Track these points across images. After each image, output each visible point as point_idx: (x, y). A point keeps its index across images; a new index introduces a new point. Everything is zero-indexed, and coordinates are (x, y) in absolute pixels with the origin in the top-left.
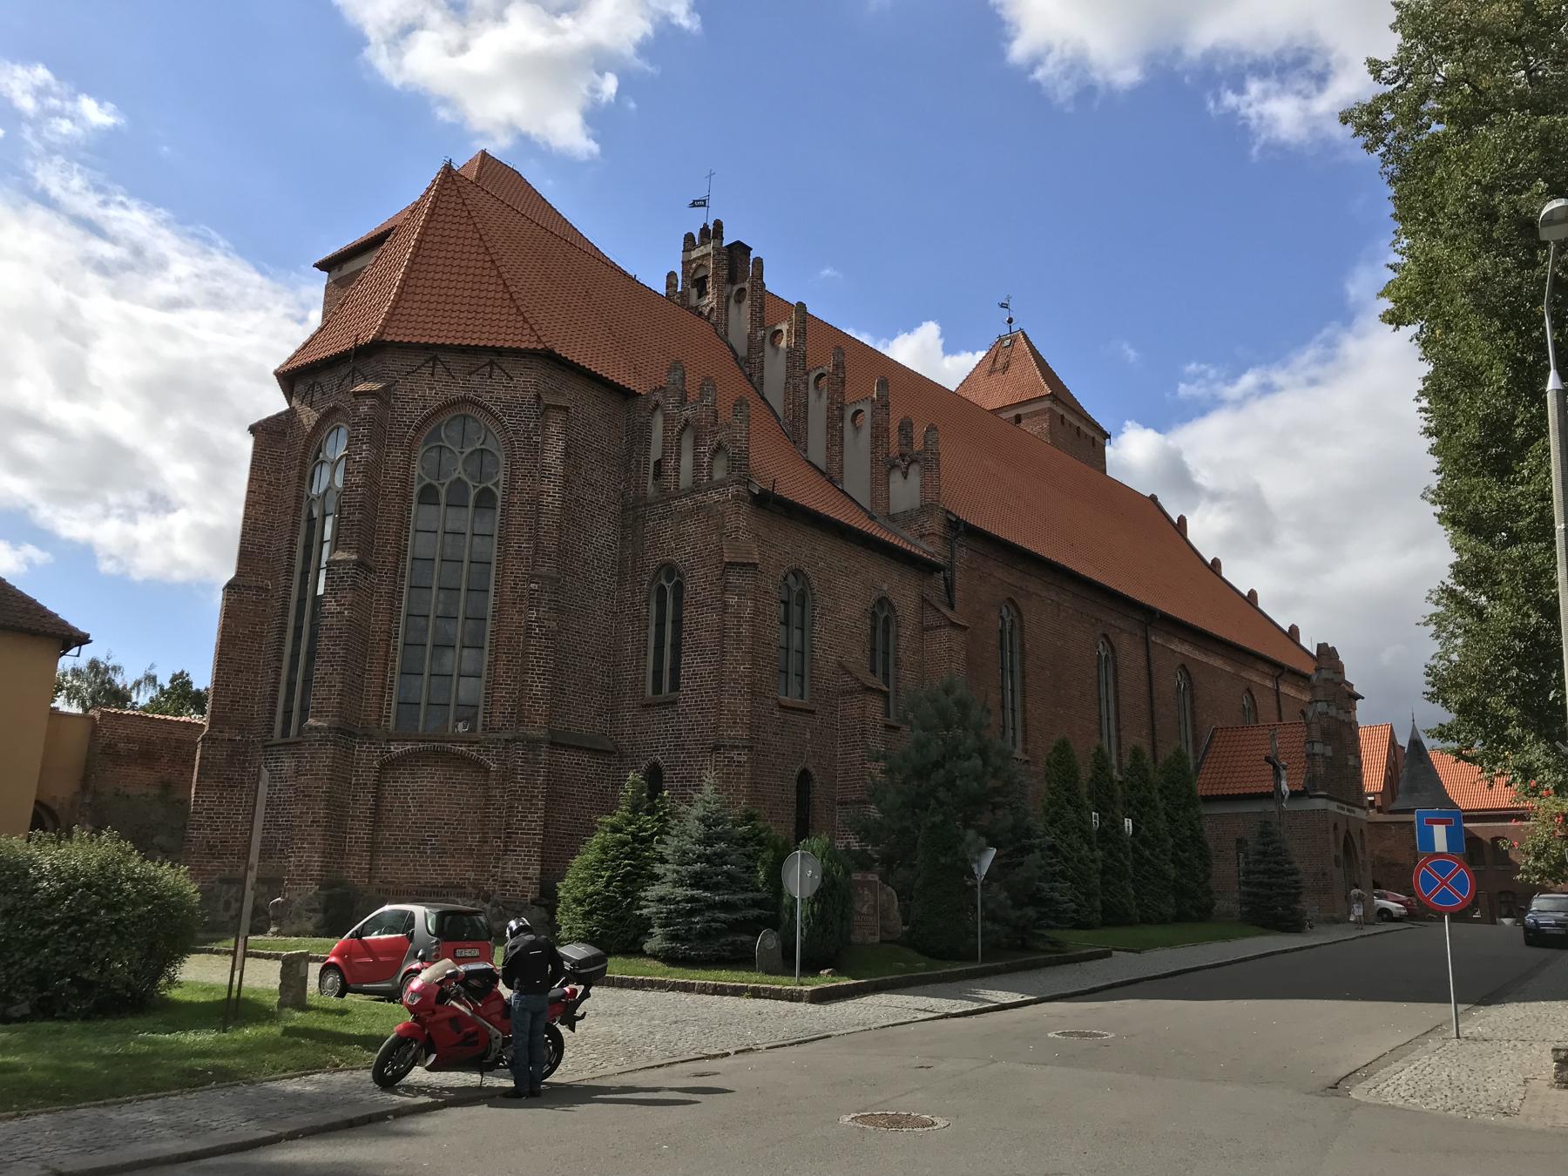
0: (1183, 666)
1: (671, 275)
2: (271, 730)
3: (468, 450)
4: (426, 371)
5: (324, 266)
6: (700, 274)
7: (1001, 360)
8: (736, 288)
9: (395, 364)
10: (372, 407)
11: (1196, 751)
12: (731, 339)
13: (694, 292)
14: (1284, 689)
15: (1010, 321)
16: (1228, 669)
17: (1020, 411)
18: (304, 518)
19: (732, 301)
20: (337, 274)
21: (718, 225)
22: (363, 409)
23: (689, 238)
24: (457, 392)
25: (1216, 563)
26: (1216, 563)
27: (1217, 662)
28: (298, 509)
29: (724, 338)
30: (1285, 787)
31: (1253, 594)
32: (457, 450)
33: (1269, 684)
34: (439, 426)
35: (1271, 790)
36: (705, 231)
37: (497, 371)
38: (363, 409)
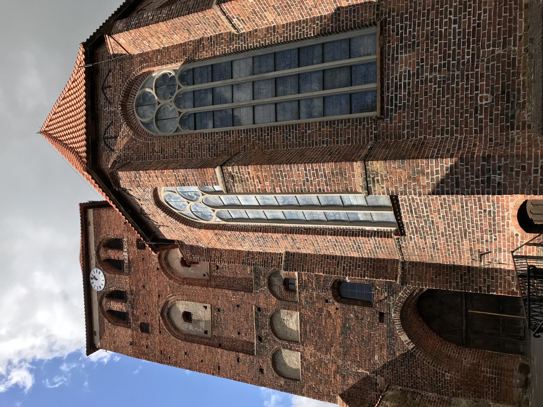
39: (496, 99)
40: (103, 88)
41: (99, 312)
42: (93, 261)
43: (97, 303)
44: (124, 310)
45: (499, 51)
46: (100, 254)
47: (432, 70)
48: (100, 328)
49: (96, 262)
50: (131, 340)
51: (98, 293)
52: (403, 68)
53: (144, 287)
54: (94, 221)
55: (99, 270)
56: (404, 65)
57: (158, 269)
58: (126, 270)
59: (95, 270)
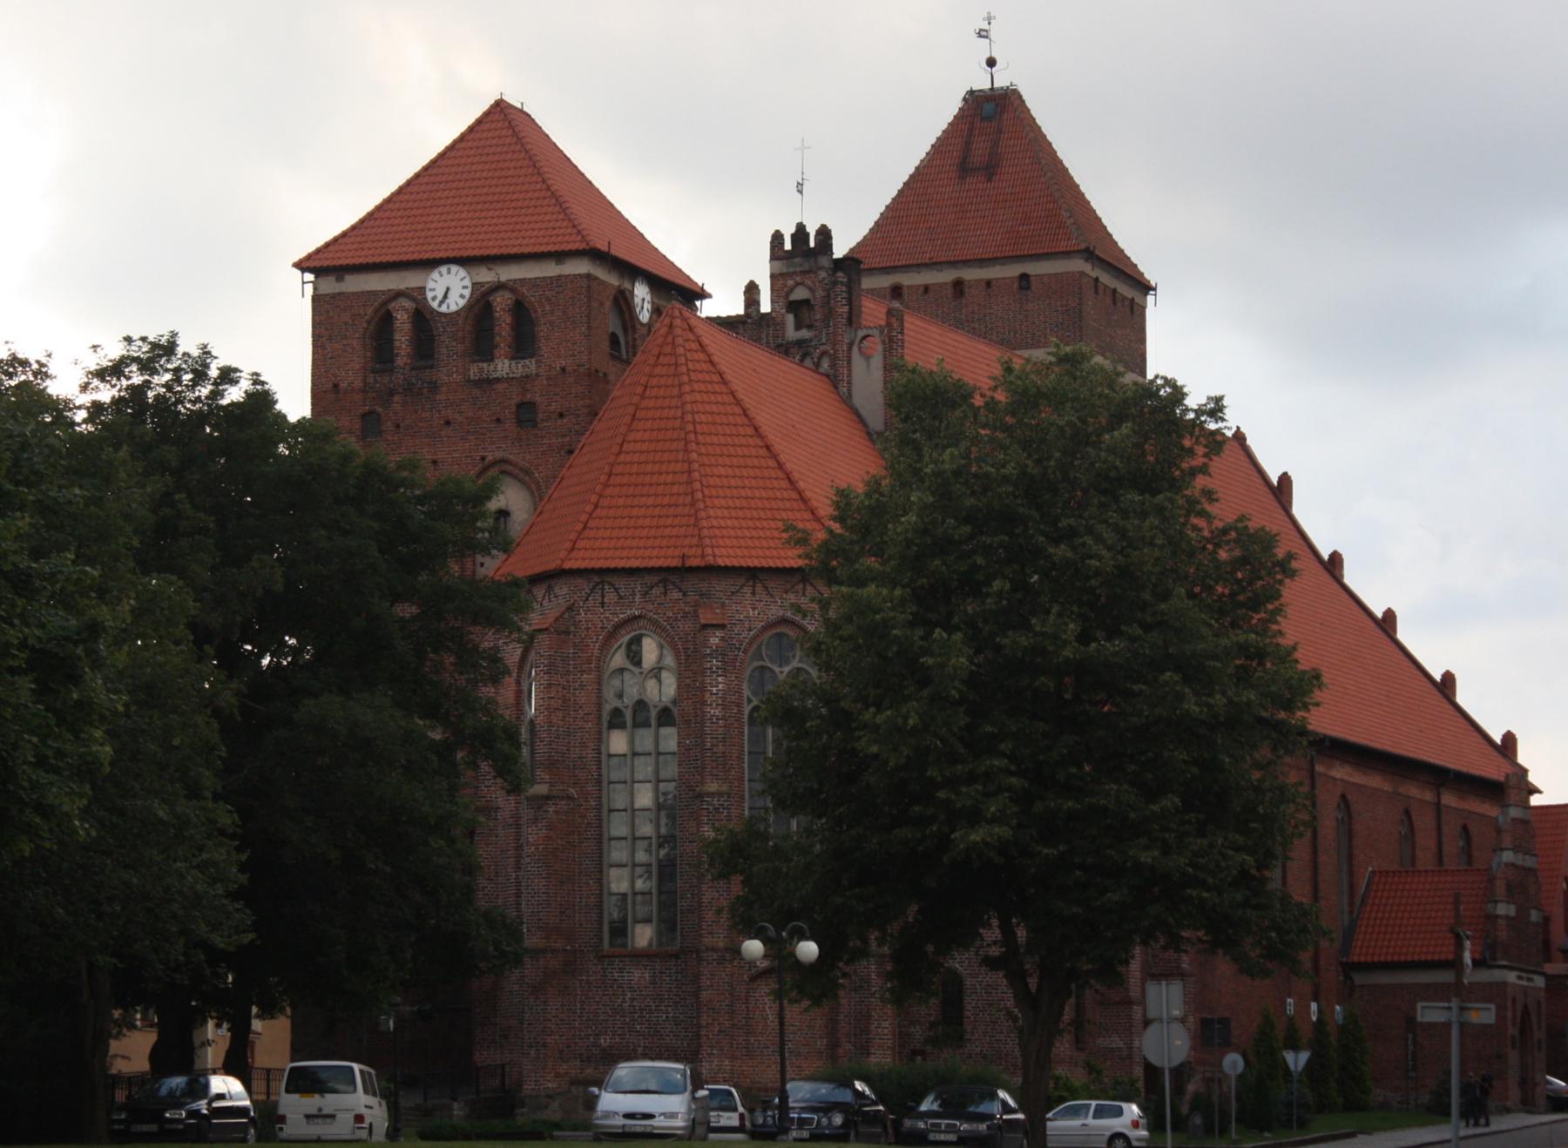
0: (1343, 796)
1: (752, 290)
2: (601, 940)
3: (786, 669)
4: (747, 590)
5: (302, 266)
6: (800, 294)
7: (980, 148)
8: (861, 334)
9: (720, 586)
10: (722, 639)
11: (1351, 904)
12: (857, 401)
13: (790, 318)
14: (1449, 799)
15: (991, 63)
16: (1387, 787)
17: (1032, 269)
18: (605, 725)
19: (855, 349)
20: (330, 286)
21: (824, 234)
22: (714, 641)
23: (777, 238)
24: (775, 612)
25: (1336, 560)
26: (1336, 560)
27: (1375, 781)
28: (600, 717)
29: (847, 401)
30: (1467, 957)
31: (1390, 616)
32: (777, 669)
33: (1429, 796)
34: (759, 647)
35: (1450, 957)
36: (800, 233)
37: (809, 588)
38: (714, 641)
39: (604, 1050)
40: (665, 581)
41: (383, 292)
42: (486, 276)
43: (402, 286)
44: (399, 362)
45: (640, 1050)
46: (500, 293)
47: (632, 1000)
48: (354, 294)
49: (482, 284)
50: (343, 385)
51: (422, 290)
52: (637, 974)
53: (448, 423)
54: (567, 276)
55: (467, 293)
56: (639, 975)
57: (483, 458)
58: (474, 371)
59: (467, 282)
